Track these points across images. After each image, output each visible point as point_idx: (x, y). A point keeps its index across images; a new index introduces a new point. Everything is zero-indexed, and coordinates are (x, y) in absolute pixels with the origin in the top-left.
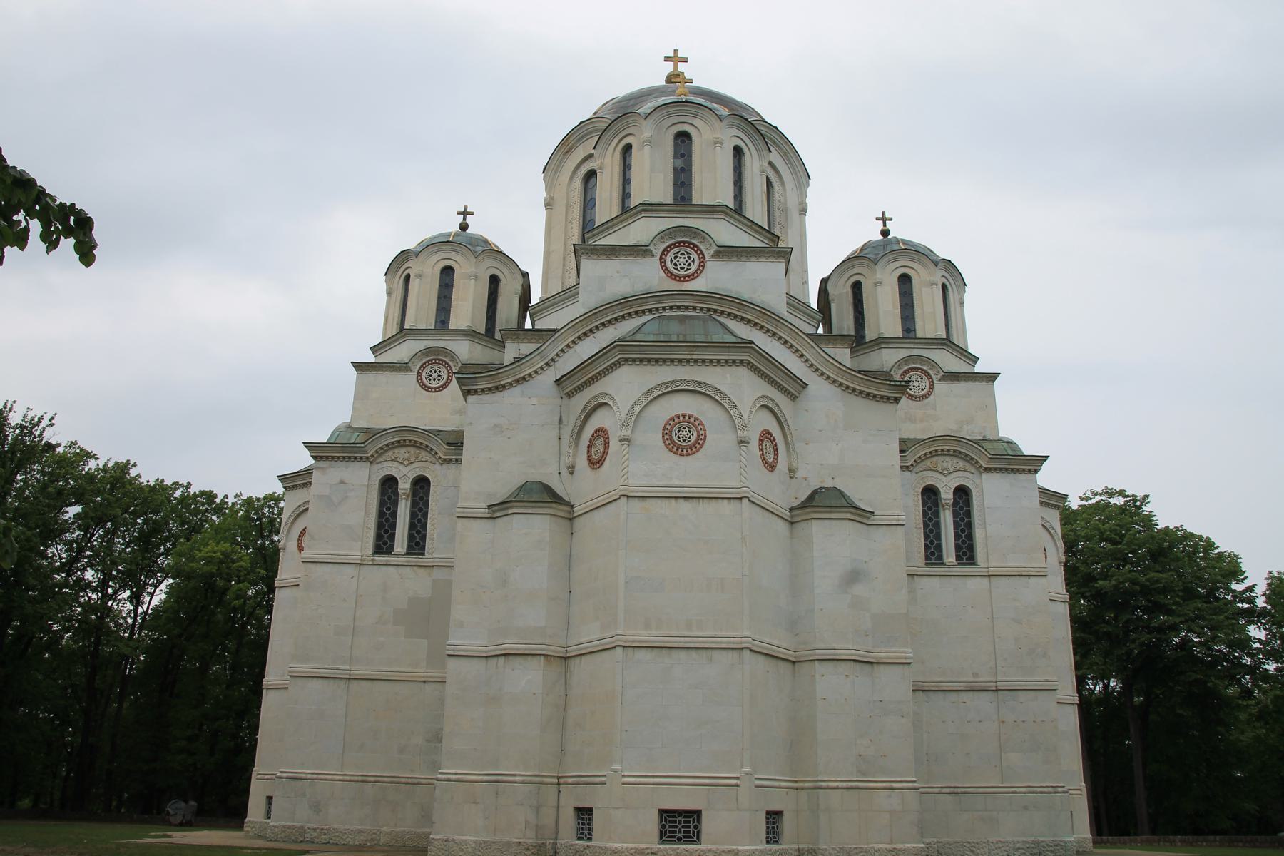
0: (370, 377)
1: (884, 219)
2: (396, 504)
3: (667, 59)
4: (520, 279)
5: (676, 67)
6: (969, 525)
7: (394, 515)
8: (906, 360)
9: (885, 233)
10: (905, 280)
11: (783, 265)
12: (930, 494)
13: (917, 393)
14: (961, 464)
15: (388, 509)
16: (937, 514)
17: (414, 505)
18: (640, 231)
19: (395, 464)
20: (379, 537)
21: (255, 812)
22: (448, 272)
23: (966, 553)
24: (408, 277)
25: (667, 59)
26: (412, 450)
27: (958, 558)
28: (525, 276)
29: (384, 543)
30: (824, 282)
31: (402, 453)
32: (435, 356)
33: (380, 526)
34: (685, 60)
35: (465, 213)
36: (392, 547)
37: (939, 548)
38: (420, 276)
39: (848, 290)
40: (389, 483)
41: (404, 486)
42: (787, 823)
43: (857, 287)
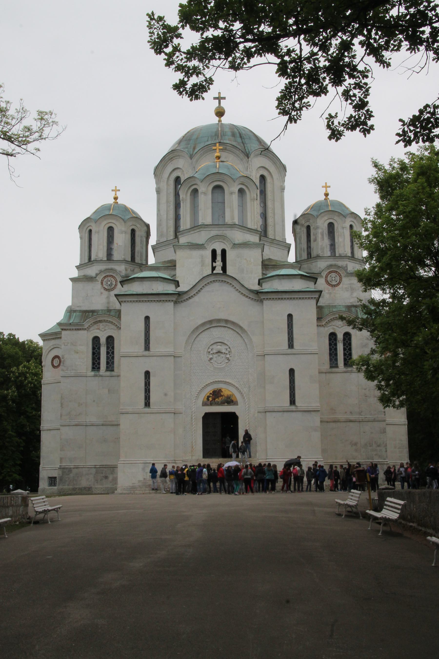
0: (80, 285)
1: (326, 187)
2: (99, 348)
3: (215, 98)
4: (145, 228)
5: (220, 103)
6: (350, 349)
7: (99, 353)
8: (331, 266)
10: (331, 226)
11: (260, 251)
12: (333, 336)
13: (334, 283)
15: (96, 351)
16: (336, 345)
17: (108, 348)
18: (200, 237)
19: (98, 331)
20: (93, 364)
21: (43, 484)
22: (111, 230)
24: (90, 231)
25: (215, 98)
26: (104, 323)
28: (148, 226)
29: (96, 366)
31: (101, 325)
32: (109, 274)
33: (93, 359)
34: (224, 98)
35: (116, 190)
36: (99, 368)
38: (98, 232)
40: (96, 340)
41: (103, 340)
43: (308, 228)
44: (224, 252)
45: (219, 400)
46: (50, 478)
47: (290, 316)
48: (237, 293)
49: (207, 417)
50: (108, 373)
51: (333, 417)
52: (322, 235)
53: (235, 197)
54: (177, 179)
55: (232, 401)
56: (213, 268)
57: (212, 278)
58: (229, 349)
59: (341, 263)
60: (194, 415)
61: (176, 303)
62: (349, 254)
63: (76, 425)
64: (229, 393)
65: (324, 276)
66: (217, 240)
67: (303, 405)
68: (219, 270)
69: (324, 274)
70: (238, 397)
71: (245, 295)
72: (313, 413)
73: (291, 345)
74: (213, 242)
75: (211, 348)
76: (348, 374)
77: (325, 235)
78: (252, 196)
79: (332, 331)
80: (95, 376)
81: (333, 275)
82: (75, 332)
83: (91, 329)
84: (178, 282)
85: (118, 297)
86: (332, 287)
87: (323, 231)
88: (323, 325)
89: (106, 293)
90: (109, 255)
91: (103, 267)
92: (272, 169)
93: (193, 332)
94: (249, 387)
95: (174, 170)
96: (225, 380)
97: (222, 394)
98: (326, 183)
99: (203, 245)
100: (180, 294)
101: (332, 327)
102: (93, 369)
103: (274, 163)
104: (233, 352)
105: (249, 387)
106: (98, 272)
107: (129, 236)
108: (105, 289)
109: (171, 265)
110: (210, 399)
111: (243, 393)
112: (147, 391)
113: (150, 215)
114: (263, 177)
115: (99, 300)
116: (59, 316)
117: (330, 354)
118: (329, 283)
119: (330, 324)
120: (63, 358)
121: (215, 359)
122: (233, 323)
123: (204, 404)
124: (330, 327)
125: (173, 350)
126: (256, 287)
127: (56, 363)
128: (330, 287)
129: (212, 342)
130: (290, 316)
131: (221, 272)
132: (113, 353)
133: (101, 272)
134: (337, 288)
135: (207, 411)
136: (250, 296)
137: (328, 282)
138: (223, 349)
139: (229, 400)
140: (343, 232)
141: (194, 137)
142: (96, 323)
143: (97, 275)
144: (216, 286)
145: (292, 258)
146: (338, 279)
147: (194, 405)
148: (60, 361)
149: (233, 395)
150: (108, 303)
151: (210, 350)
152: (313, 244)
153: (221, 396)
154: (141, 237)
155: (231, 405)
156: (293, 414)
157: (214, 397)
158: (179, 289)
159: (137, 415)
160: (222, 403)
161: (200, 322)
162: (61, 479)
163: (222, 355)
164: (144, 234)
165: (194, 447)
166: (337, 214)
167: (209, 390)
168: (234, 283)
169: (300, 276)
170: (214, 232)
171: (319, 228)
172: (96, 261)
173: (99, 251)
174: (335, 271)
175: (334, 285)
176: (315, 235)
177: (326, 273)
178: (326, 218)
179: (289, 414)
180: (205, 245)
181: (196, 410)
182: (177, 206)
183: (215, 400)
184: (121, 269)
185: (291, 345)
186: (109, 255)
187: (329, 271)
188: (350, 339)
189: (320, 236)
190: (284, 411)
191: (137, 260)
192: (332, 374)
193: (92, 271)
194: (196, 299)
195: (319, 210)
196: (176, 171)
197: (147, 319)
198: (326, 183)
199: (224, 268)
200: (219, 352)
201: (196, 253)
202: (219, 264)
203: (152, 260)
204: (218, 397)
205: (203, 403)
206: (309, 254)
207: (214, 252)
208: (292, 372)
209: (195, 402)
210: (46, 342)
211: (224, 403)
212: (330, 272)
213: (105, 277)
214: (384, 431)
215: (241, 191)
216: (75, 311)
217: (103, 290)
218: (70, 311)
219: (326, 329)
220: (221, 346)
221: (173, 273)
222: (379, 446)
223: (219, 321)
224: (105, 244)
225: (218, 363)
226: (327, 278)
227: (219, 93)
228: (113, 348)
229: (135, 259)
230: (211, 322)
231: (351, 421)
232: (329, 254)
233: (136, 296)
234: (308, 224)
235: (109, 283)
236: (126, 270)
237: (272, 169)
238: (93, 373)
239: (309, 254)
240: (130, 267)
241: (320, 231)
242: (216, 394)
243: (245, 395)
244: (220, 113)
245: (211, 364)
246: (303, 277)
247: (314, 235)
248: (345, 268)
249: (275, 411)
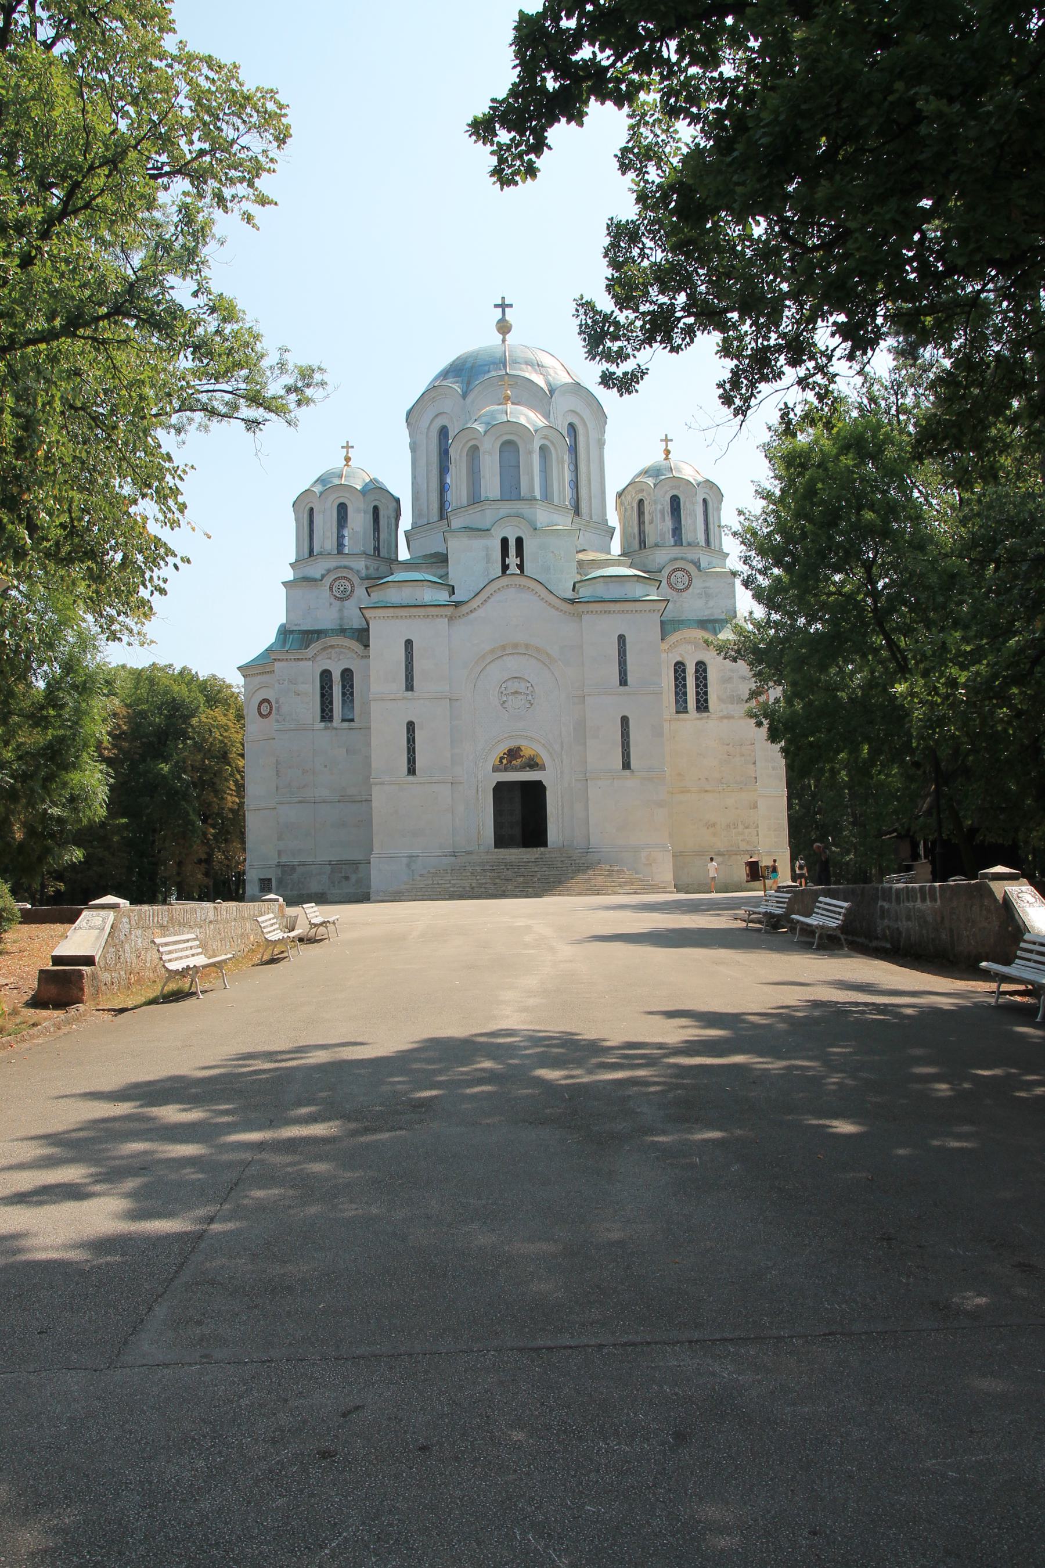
1: (667, 440)
2: (331, 687)
3: (496, 306)
4: (395, 504)
9: (667, 452)
10: (675, 501)
12: (680, 668)
13: (680, 586)
16: (684, 679)
17: (344, 687)
19: (329, 661)
20: (323, 711)
21: (251, 888)
22: (342, 508)
23: (703, 706)
24: (311, 510)
25: (496, 306)
27: (698, 709)
28: (398, 501)
29: (326, 715)
30: (620, 495)
34: (511, 306)
39: (635, 505)
40: (326, 675)
41: (336, 676)
43: (641, 501)
44: (519, 541)
45: (516, 763)
46: (262, 880)
47: (622, 639)
49: (500, 789)
50: (346, 724)
52: (662, 512)
53: (536, 457)
54: (443, 432)
55: (537, 764)
56: (505, 567)
57: (505, 581)
59: (690, 556)
62: (703, 543)
63: (300, 802)
64: (532, 753)
68: (513, 569)
69: (665, 573)
70: (545, 757)
71: (554, 606)
73: (623, 682)
75: (504, 686)
76: (704, 721)
79: (679, 659)
80: (326, 728)
81: (679, 574)
82: (293, 664)
83: (318, 658)
84: (453, 587)
85: (364, 611)
89: (338, 603)
90: (340, 545)
91: (332, 563)
92: (586, 414)
94: (562, 743)
95: (437, 416)
99: (488, 530)
100: (458, 604)
102: (323, 718)
105: (562, 743)
106: (324, 572)
107: (370, 517)
108: (336, 597)
109: (441, 559)
110: (505, 761)
112: (411, 750)
113: (400, 483)
114: (571, 426)
115: (325, 614)
116: (268, 637)
117: (677, 694)
120: (277, 702)
121: (510, 702)
122: (537, 649)
123: (495, 769)
126: (570, 594)
127: (265, 709)
128: (675, 593)
130: (622, 639)
131: (519, 572)
132: (352, 694)
133: (329, 571)
138: (522, 687)
141: (469, 365)
142: (324, 649)
143: (323, 576)
145: (616, 547)
148: (271, 708)
149: (538, 755)
150: (341, 619)
152: (647, 527)
153: (521, 757)
154: (388, 517)
158: (454, 598)
160: (522, 768)
162: (280, 881)
163: (520, 697)
164: (393, 514)
167: (503, 748)
168: (539, 588)
170: (503, 512)
172: (320, 554)
173: (325, 539)
180: (492, 531)
181: (484, 778)
182: (443, 470)
184: (360, 564)
185: (623, 682)
186: (340, 545)
188: (705, 671)
189: (659, 515)
191: (384, 553)
193: (316, 569)
194: (480, 613)
195: (657, 476)
196: (440, 418)
197: (409, 643)
199: (521, 567)
200: (516, 692)
201: (478, 544)
202: (513, 560)
203: (404, 554)
204: (516, 759)
206: (643, 544)
207: (505, 542)
208: (625, 721)
210: (248, 679)
213: (335, 580)
214: (755, 807)
215: (543, 449)
216: (292, 632)
217: (332, 600)
218: (284, 632)
221: (442, 572)
222: (747, 828)
223: (516, 646)
224: (335, 530)
227: (503, 298)
228: (352, 686)
229: (381, 553)
230: (504, 647)
231: (706, 791)
233: (392, 610)
235: (342, 589)
236: (367, 568)
237: (586, 414)
238: (323, 725)
239: (643, 544)
240: (373, 564)
242: (513, 753)
244: (504, 327)
248: (697, 565)
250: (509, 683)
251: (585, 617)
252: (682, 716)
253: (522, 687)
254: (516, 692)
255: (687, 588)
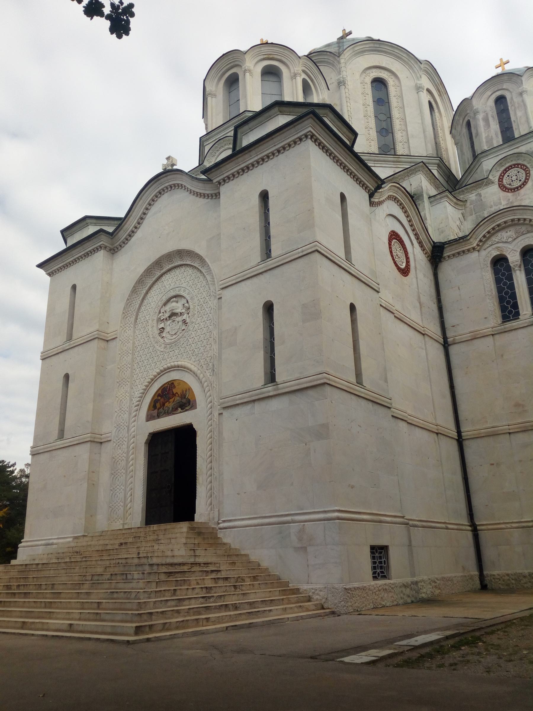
13: (516, 184)
14: (524, 228)
16: (510, 278)
37: (515, 306)
42: (396, 559)
45: (170, 405)
47: (264, 196)
48: (192, 198)
51: (520, 421)
52: (486, 120)
55: (189, 402)
58: (186, 305)
60: (132, 440)
61: (113, 251)
65: (497, 180)
66: (221, 150)
67: (289, 378)
72: (311, 392)
74: (217, 153)
77: (491, 119)
78: (292, 71)
79: (495, 253)
81: (513, 172)
86: (515, 191)
87: (487, 114)
88: (474, 249)
93: (134, 290)
96: (176, 363)
97: (175, 391)
98: (501, 60)
101: (494, 247)
103: (398, 58)
104: (191, 307)
110: (158, 405)
111: (203, 380)
117: (501, 299)
118: (506, 188)
119: (489, 243)
121: (168, 329)
123: (150, 418)
124: (490, 249)
125: (97, 327)
128: (510, 195)
129: (164, 299)
134: (522, 191)
135: (152, 431)
136: (207, 192)
137: (505, 187)
139: (184, 401)
140: (523, 101)
144: (165, 199)
146: (522, 175)
147: (135, 421)
149: (190, 389)
151: (160, 315)
153: (174, 395)
155: (186, 410)
156: (275, 404)
157: (162, 400)
159: (47, 455)
160: (173, 411)
161: (141, 270)
165: (129, 506)
166: (506, 77)
169: (276, 109)
171: (478, 112)
174: (514, 165)
175: (517, 188)
176: (476, 127)
177: (500, 172)
178: (489, 93)
179: (263, 404)
183: (164, 405)
187: (504, 168)
189: (481, 123)
190: (254, 401)
192: (506, 334)
194: (139, 234)
198: (501, 60)
205: (147, 415)
209: (135, 416)
211: (177, 409)
212: (505, 171)
219: (483, 253)
220: (177, 302)
225: (172, 335)
226: (502, 181)
230: (158, 263)
232: (498, 140)
234: (466, 120)
241: (480, 116)
243: (205, 384)
245: (162, 340)
246: (284, 109)
247: (474, 128)
249: (238, 405)
250: (168, 308)
251: (224, 189)
252: (514, 324)
253: (177, 306)
254: (173, 314)
255: (525, 183)
